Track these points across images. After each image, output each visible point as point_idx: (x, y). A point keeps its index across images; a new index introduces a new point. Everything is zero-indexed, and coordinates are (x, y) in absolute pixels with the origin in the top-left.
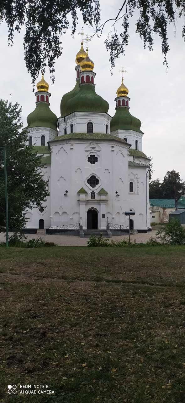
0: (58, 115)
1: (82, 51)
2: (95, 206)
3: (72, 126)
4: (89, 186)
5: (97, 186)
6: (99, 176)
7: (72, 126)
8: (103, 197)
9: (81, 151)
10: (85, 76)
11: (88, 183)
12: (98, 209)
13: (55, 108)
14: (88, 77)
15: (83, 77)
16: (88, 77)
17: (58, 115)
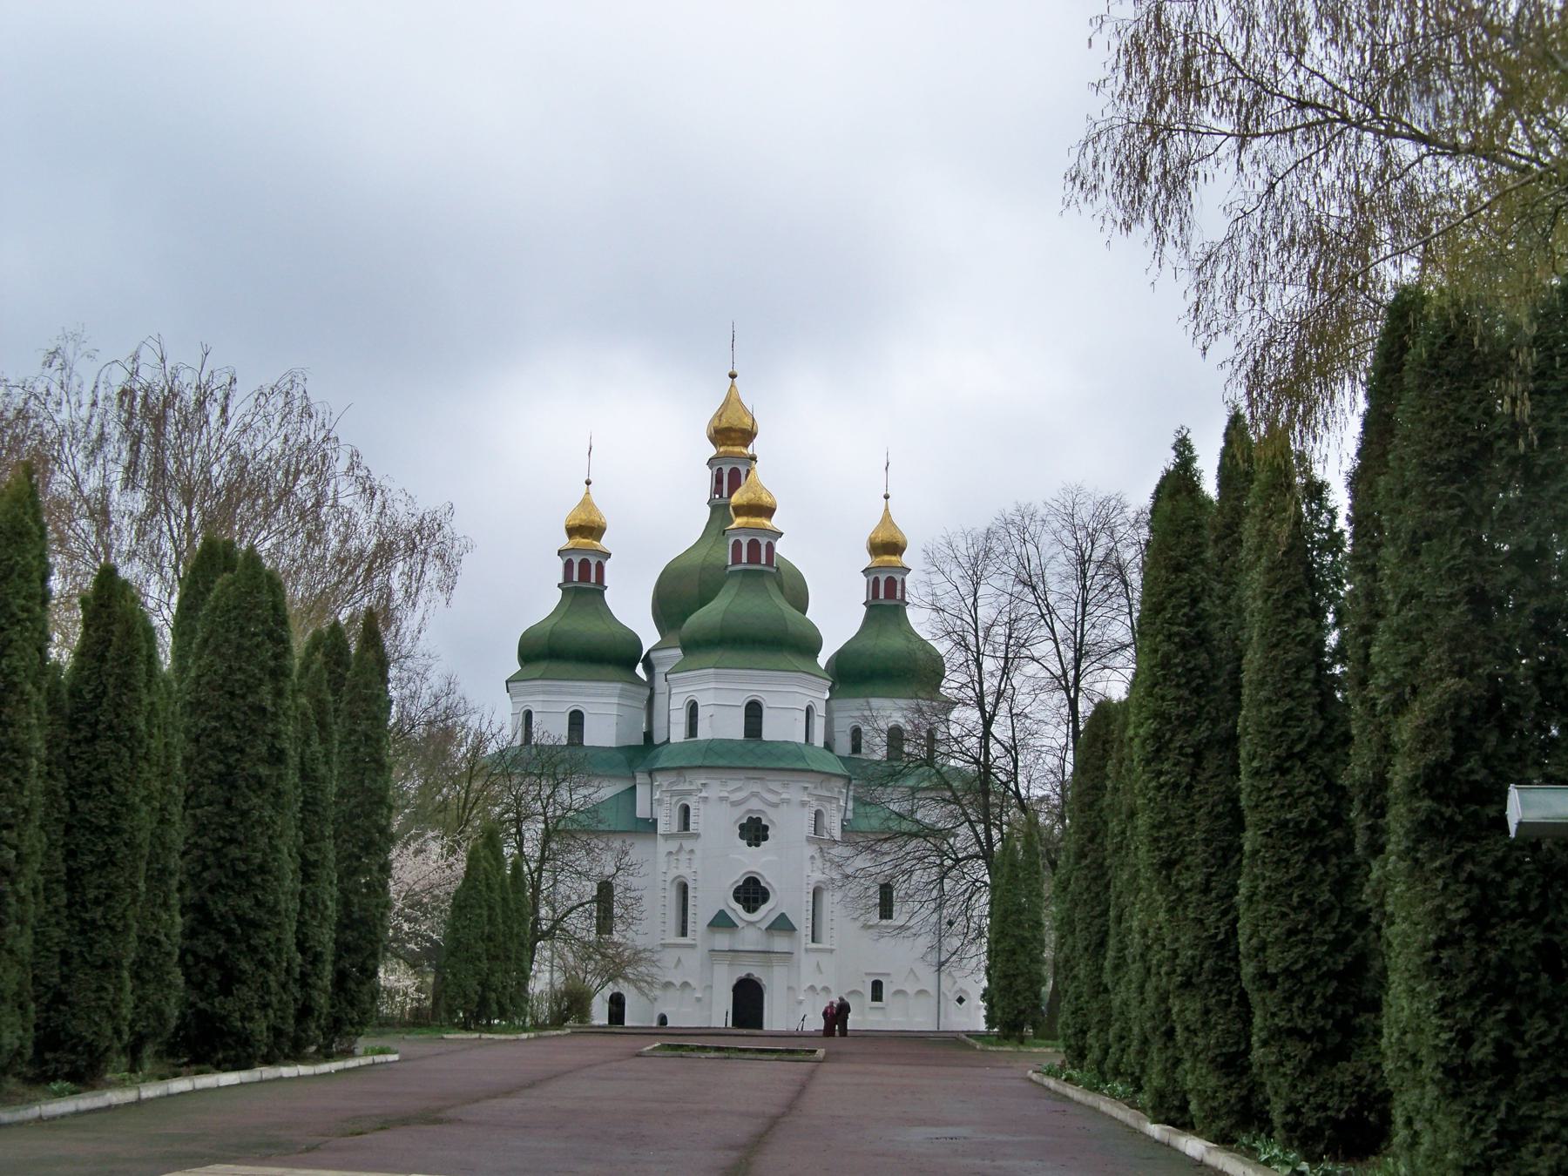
0: (649, 636)
1: (732, 401)
2: (757, 973)
3: (693, 709)
4: (739, 907)
5: (764, 909)
6: (768, 879)
7: (693, 709)
8: (780, 943)
9: (718, 804)
10: (745, 541)
11: (737, 899)
12: (764, 982)
13: (631, 605)
14: (754, 545)
15: (737, 545)
16: (754, 545)
17: (649, 636)
